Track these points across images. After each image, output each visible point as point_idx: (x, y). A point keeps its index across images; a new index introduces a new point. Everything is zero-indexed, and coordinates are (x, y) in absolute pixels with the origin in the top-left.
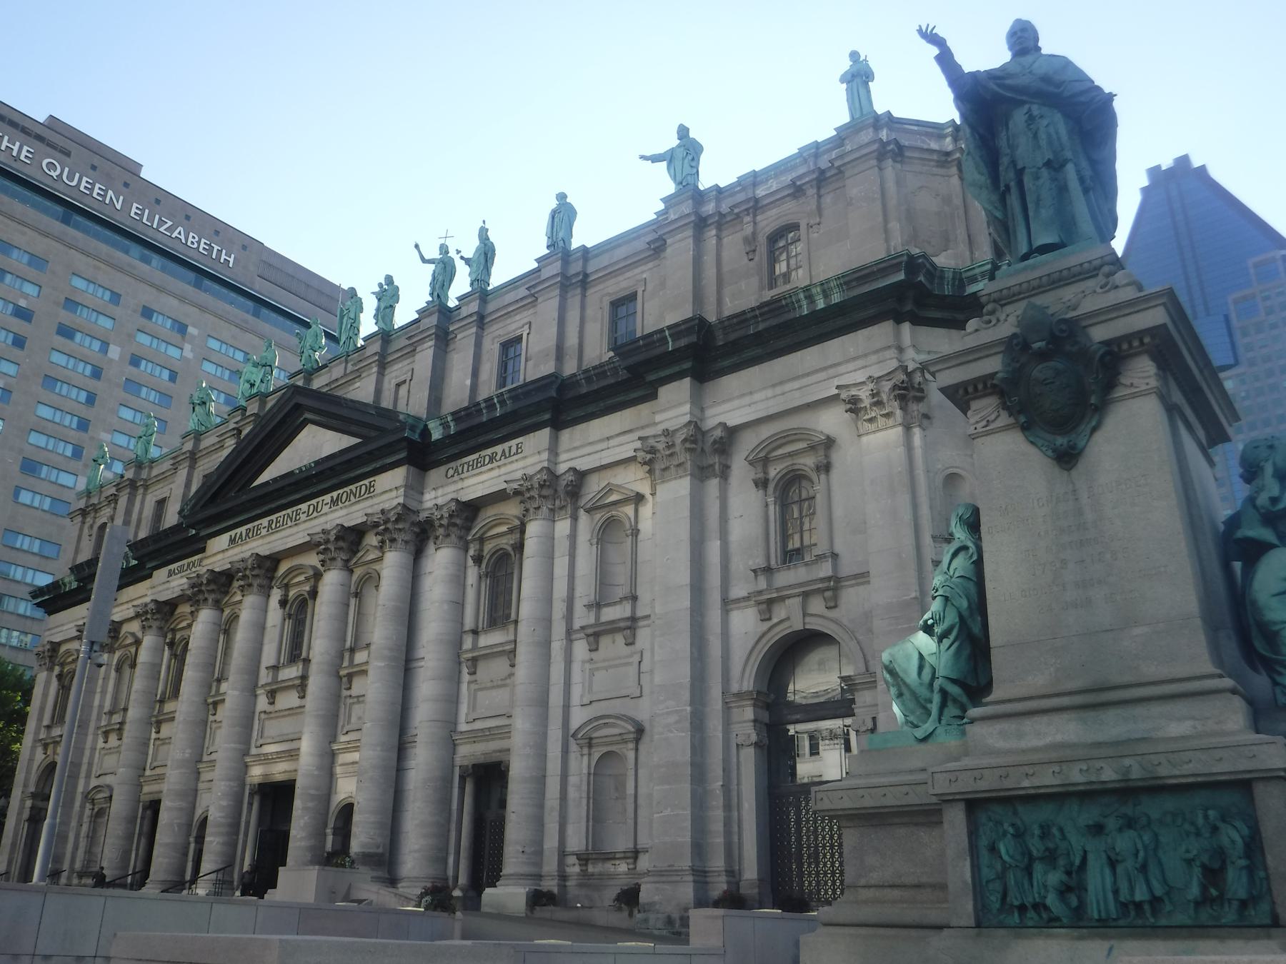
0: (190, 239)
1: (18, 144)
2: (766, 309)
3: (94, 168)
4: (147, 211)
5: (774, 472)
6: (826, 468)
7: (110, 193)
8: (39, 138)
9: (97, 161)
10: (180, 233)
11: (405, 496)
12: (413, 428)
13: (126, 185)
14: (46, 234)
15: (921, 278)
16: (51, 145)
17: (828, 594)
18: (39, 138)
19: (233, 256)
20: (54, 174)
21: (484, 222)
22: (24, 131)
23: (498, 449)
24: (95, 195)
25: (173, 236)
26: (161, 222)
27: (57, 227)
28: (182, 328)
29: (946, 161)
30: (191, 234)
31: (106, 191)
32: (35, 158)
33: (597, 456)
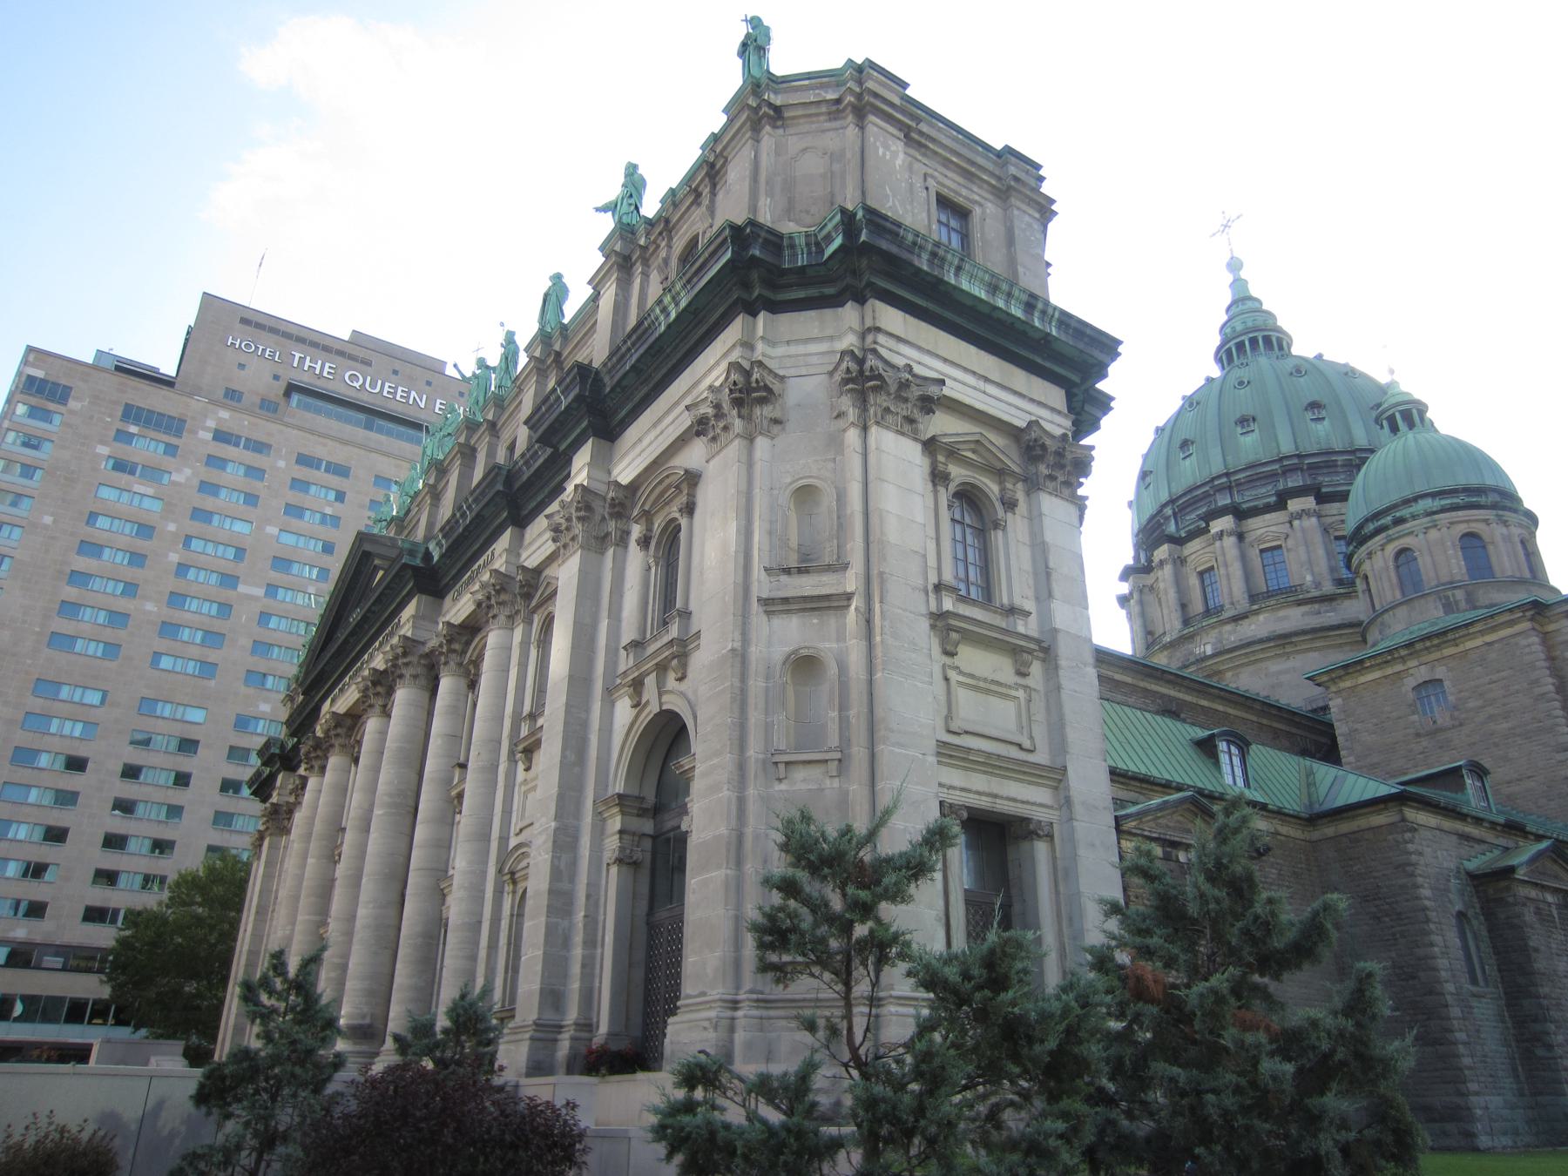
1: (320, 362)
2: (634, 337)
3: (395, 372)
5: (658, 524)
6: (690, 509)
7: (413, 394)
8: (341, 353)
9: (397, 365)
11: (414, 627)
12: (412, 553)
13: (429, 383)
14: (345, 443)
15: (757, 253)
16: (352, 358)
17: (675, 662)
18: (341, 353)
20: (357, 385)
21: (502, 324)
22: (326, 349)
23: (481, 562)
27: (360, 433)
29: (838, 111)
31: (409, 393)
32: (335, 372)
33: (543, 549)
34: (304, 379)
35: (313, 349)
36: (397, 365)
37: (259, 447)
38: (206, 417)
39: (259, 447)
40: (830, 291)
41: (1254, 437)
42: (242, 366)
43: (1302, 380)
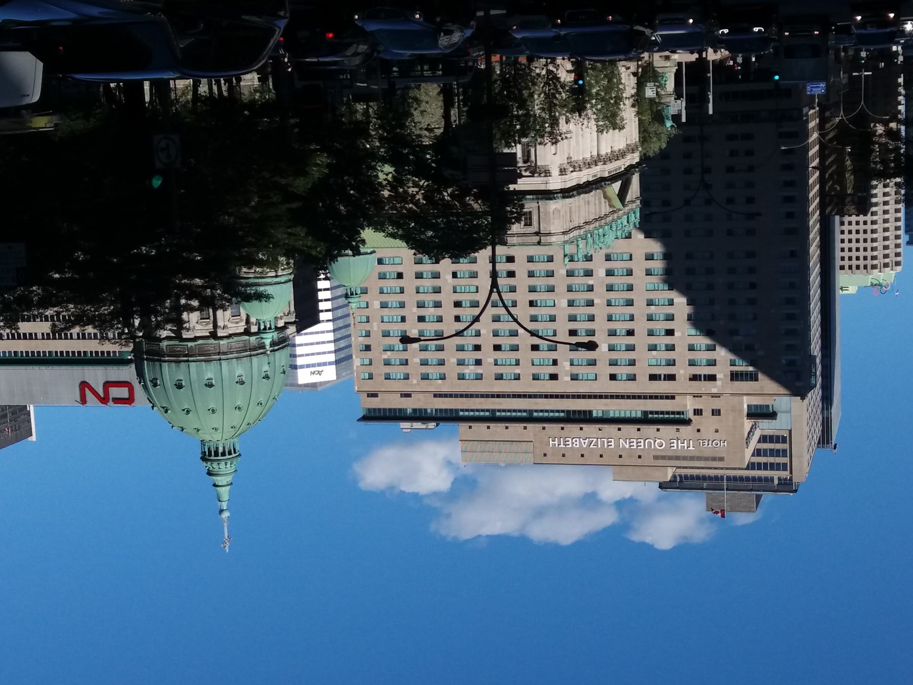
0: (578, 443)
1: (680, 448)
3: (640, 457)
4: (606, 446)
7: (627, 447)
9: (639, 462)
10: (585, 443)
12: (608, 184)
16: (663, 458)
19: (551, 446)
20: (658, 441)
24: (635, 440)
25: (587, 439)
26: (596, 445)
28: (574, 378)
30: (578, 446)
34: (683, 428)
35: (685, 454)
36: (639, 462)
37: (695, 378)
38: (722, 386)
39: (695, 378)
40: (554, 191)
41: (264, 370)
42: (717, 431)
43: (239, 404)
